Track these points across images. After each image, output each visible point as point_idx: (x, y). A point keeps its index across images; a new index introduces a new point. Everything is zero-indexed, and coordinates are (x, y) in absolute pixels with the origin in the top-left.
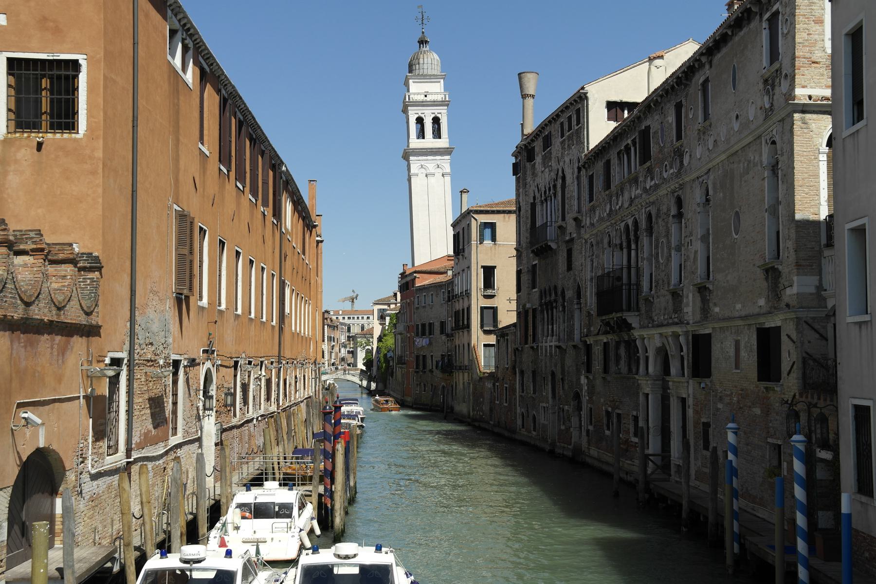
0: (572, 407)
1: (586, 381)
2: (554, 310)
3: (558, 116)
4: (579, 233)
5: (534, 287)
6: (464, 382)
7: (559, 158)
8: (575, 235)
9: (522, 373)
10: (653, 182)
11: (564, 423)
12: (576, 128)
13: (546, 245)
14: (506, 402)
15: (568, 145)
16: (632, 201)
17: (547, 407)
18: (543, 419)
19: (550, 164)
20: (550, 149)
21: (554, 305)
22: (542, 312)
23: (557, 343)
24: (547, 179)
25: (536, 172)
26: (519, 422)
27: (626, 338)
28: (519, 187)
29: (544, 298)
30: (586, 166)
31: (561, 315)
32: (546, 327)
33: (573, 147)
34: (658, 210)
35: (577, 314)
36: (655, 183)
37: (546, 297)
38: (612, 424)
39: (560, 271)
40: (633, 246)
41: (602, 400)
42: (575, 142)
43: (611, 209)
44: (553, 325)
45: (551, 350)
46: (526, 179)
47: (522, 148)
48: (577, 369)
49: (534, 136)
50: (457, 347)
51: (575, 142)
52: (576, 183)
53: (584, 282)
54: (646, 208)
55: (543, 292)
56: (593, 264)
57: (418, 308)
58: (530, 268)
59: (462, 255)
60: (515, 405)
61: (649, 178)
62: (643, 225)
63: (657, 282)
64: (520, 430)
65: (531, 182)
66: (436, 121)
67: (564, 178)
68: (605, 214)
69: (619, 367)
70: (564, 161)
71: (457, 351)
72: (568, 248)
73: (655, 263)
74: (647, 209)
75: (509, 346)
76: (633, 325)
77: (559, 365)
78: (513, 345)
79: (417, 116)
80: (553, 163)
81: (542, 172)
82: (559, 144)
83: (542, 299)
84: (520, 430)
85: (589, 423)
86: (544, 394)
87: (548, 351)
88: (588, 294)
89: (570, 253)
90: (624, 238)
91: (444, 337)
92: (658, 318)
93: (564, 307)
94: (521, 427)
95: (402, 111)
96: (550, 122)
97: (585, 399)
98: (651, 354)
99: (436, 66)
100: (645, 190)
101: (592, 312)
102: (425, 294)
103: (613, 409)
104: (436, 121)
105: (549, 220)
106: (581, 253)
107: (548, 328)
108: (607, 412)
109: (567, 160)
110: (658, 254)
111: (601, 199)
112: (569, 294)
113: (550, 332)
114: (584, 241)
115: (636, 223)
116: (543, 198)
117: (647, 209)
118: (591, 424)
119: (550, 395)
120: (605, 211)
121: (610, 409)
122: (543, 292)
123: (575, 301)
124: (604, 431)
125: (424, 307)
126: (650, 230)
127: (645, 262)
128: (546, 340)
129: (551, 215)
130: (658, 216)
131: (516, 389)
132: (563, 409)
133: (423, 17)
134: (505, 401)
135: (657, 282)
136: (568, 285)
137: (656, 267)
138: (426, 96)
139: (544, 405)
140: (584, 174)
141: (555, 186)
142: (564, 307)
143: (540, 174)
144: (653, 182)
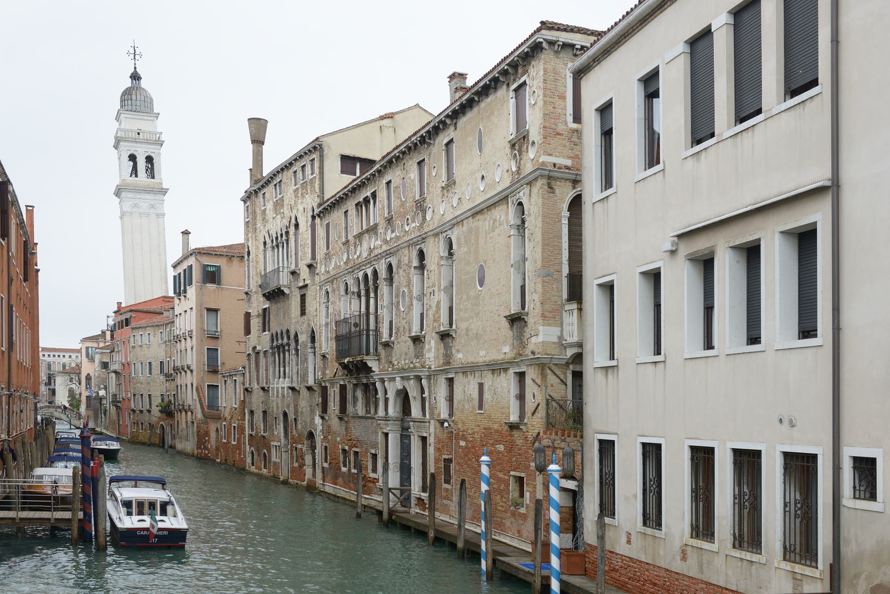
0: (305, 446)
1: (321, 421)
2: (287, 353)
3: (291, 164)
4: (313, 280)
5: (264, 331)
6: (187, 421)
7: (292, 206)
8: (307, 282)
9: (252, 413)
10: (394, 235)
11: (297, 461)
12: (311, 177)
13: (279, 289)
14: (234, 441)
15: (302, 194)
16: (371, 251)
17: (279, 446)
18: (275, 457)
19: (282, 211)
20: (283, 197)
21: (287, 348)
22: (273, 354)
23: (290, 385)
24: (279, 225)
25: (267, 218)
26: (249, 460)
27: (364, 381)
28: (248, 231)
29: (275, 341)
30: (322, 215)
31: (294, 358)
32: (277, 369)
33: (307, 196)
34: (399, 261)
35: (311, 357)
36: (396, 236)
37: (277, 341)
38: (350, 462)
39: (293, 315)
40: (372, 295)
41: (338, 439)
42: (309, 191)
43: (348, 258)
44: (284, 367)
45: (283, 391)
46: (255, 224)
47: (251, 193)
48: (311, 410)
49: (265, 183)
50: (179, 387)
51: (309, 191)
52: (310, 231)
53: (318, 327)
54: (386, 259)
55: (274, 336)
56: (328, 310)
57: (134, 347)
58: (260, 312)
59: (185, 296)
60: (245, 444)
61: (389, 231)
62: (383, 274)
63: (398, 329)
64: (250, 467)
65: (262, 227)
66: (149, 160)
67: (297, 226)
68: (342, 263)
69: (356, 408)
70: (298, 209)
71: (179, 391)
72: (302, 294)
73: (395, 311)
74: (388, 260)
75: (237, 386)
76: (373, 369)
77: (292, 406)
78: (242, 386)
79: (129, 153)
80: (286, 210)
81: (274, 218)
82: (292, 192)
83: (273, 342)
84: (250, 467)
85: (323, 461)
86: (276, 433)
87: (280, 392)
88: (323, 338)
89: (303, 297)
90: (362, 286)
91: (162, 378)
92: (398, 363)
93: (297, 350)
94: (250, 465)
95: (114, 147)
96: (282, 169)
97: (319, 438)
98: (391, 395)
99: (149, 104)
100: (386, 242)
101: (327, 356)
102: (141, 333)
103: (351, 447)
104: (149, 160)
105: (281, 265)
106: (315, 299)
107: (280, 370)
108: (344, 451)
109: (301, 208)
110: (398, 302)
111: (338, 248)
112: (303, 338)
113: (282, 374)
114: (318, 288)
115: (375, 273)
116: (275, 244)
117: (388, 260)
118: (326, 461)
119: (282, 434)
120: (343, 259)
121: (347, 448)
122: (274, 336)
123: (309, 345)
124: (340, 469)
125: (141, 346)
126: (390, 280)
127: (385, 309)
128: (278, 381)
129: (283, 261)
130: (399, 267)
131: (245, 428)
132: (296, 448)
134: (233, 440)
135: (398, 329)
136: (301, 329)
137: (396, 315)
138: (139, 134)
139: (276, 443)
140: (319, 223)
141: (287, 233)
142: (297, 350)
143: (271, 220)
144: (394, 235)
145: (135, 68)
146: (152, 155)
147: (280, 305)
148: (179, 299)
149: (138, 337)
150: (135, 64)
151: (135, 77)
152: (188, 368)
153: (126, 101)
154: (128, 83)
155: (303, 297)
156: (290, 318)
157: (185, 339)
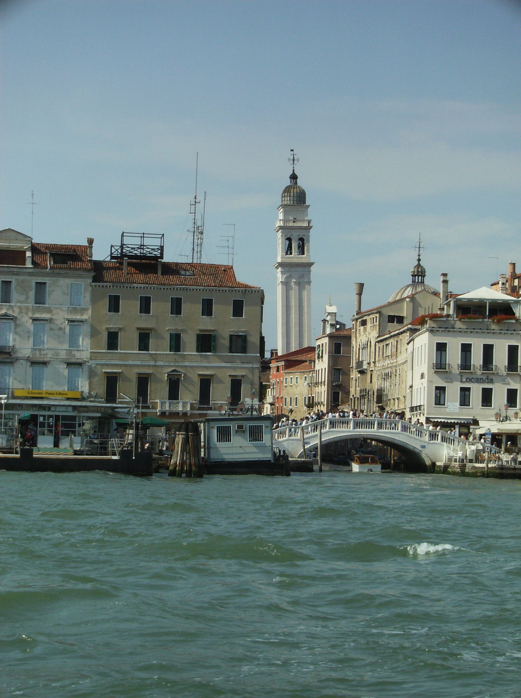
4: (375, 369)
8: (373, 369)
57: (286, 386)
59: (322, 360)
60: (348, 444)
67: (370, 342)
89: (371, 375)
104: (302, 240)
133: (294, 158)
141: (367, 344)
145: (294, 170)
146: (304, 237)
147: (364, 376)
148: (319, 361)
149: (289, 380)
150: (293, 168)
151: (294, 177)
152: (322, 403)
153: (286, 198)
154: (287, 182)
155: (371, 375)
156: (367, 383)
157: (321, 386)
